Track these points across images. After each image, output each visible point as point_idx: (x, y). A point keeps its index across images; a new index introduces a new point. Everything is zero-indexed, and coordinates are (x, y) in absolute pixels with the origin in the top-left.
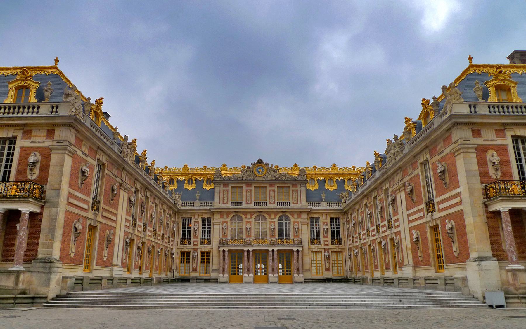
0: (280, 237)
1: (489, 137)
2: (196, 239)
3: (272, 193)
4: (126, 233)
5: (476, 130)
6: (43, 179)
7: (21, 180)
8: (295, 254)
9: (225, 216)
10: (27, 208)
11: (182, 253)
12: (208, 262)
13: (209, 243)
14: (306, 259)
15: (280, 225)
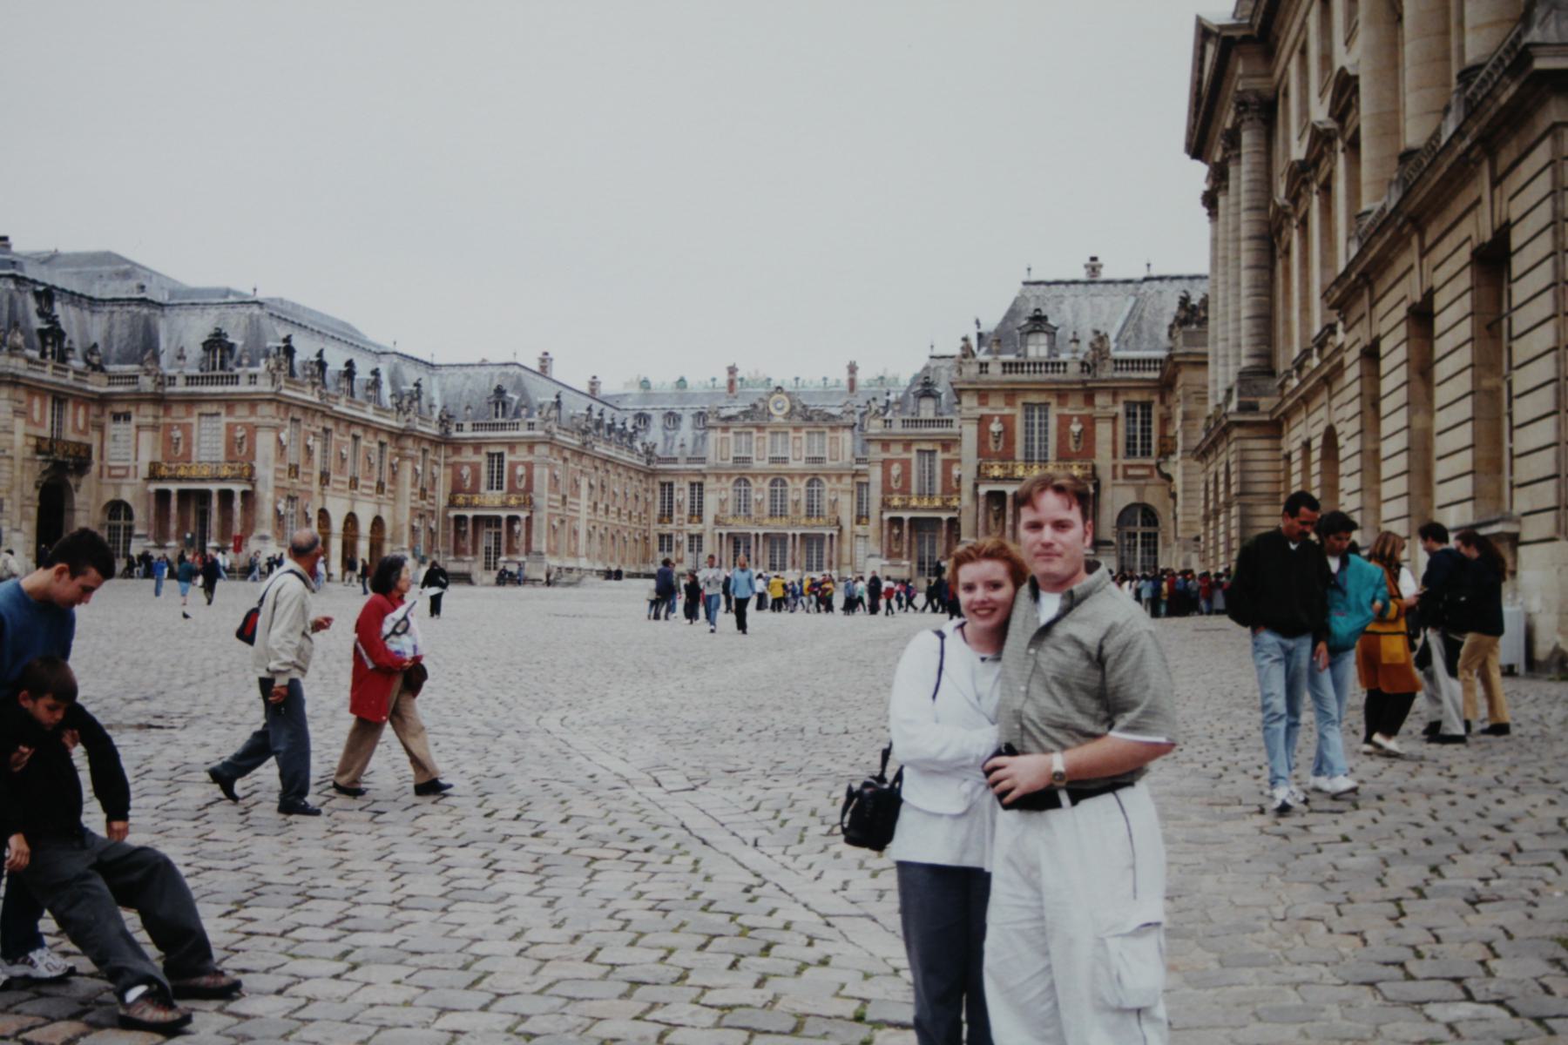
0: (809, 516)
1: (896, 451)
2: (681, 515)
3: (798, 444)
4: (589, 521)
5: (886, 444)
6: (529, 488)
7: (512, 490)
8: (827, 540)
9: (724, 479)
10: (523, 515)
11: (661, 537)
12: (700, 550)
13: (701, 521)
14: (846, 548)
15: (810, 494)
